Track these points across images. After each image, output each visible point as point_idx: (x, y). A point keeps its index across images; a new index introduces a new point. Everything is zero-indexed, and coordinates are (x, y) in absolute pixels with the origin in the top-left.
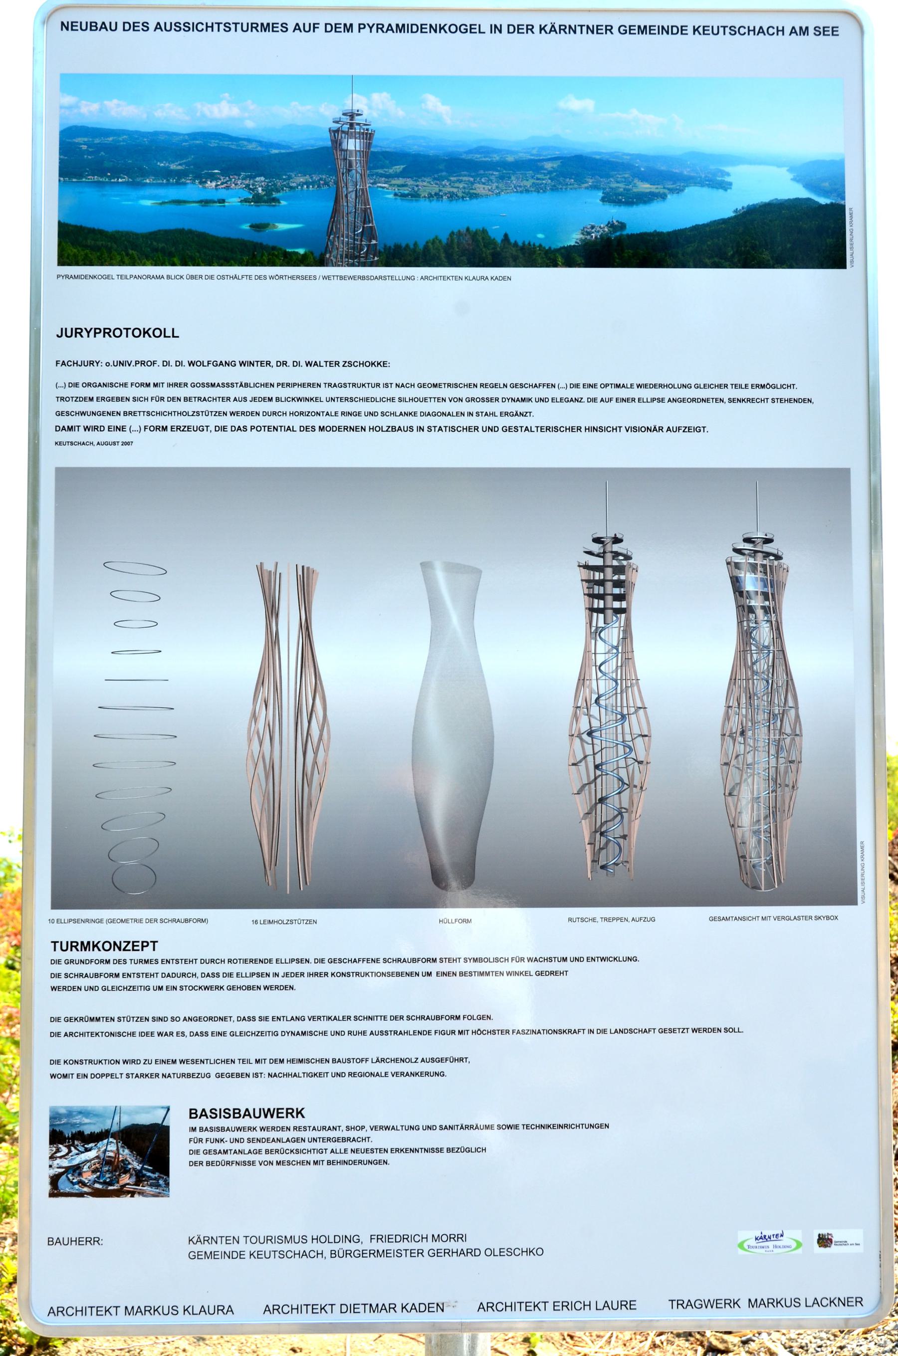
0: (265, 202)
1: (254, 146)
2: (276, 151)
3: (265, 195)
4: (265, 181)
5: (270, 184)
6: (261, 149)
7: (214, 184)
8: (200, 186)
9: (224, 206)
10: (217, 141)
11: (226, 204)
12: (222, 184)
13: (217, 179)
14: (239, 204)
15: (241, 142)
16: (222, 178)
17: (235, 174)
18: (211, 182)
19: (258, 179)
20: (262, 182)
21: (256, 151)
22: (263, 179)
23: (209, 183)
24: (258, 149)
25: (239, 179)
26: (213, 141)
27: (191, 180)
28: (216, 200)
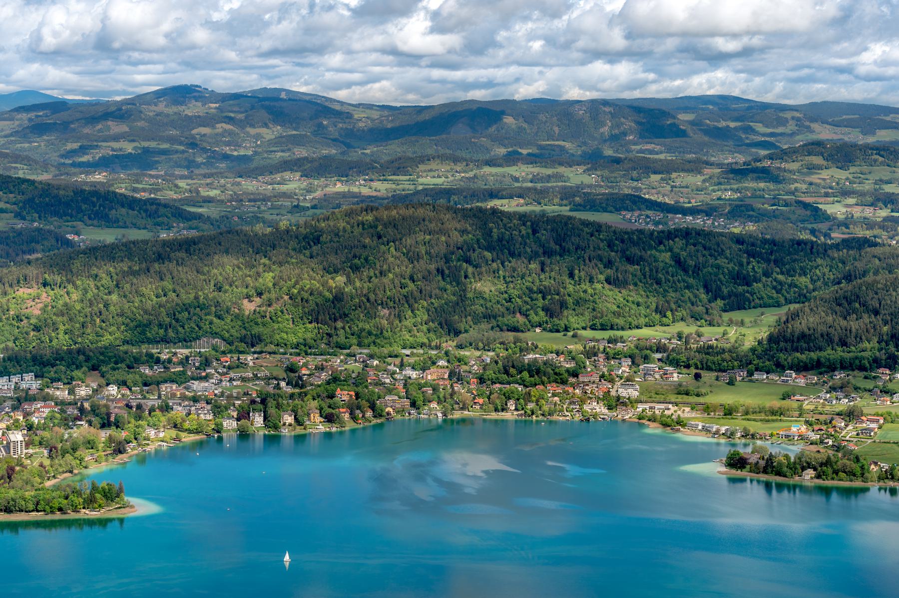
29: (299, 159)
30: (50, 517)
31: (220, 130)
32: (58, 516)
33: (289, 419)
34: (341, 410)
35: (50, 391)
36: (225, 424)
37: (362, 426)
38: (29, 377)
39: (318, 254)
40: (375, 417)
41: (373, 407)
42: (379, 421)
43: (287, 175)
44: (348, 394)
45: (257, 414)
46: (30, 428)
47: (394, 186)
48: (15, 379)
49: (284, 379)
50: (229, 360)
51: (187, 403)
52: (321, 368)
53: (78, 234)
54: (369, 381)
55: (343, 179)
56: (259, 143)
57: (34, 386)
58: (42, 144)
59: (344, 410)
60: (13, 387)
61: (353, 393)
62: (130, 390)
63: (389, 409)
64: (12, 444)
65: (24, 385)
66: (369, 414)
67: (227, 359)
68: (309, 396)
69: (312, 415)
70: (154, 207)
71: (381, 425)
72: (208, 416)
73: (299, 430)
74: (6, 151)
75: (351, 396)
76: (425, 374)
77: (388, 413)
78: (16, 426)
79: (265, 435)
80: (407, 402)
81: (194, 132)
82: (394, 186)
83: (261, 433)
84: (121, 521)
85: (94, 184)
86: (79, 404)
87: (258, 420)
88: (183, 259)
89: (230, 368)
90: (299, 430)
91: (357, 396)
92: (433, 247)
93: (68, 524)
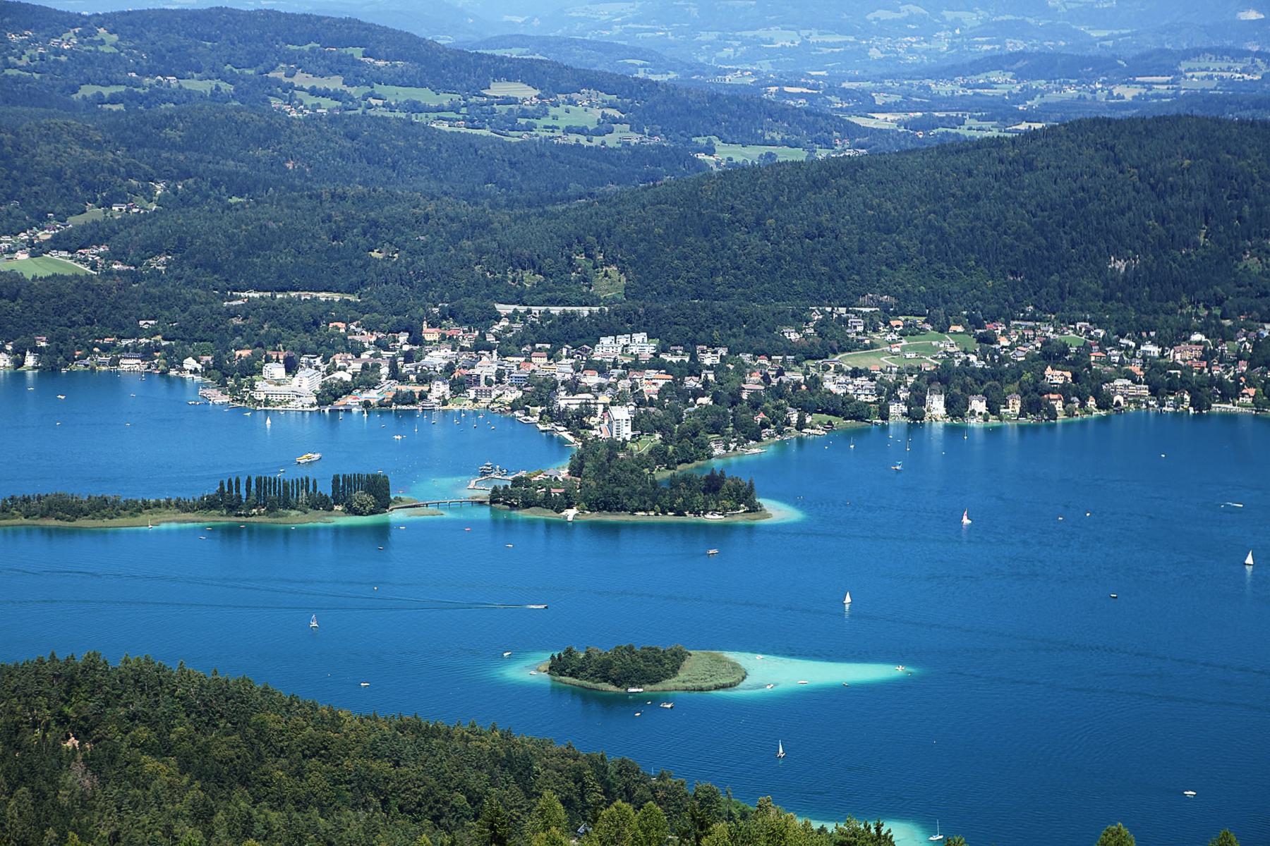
0: (654, 498)
1: (591, 117)
2: (747, 155)
3: (659, 456)
4: (656, 364)
5: (692, 382)
6: (635, 139)
7: (307, 382)
8: (219, 398)
9: (383, 531)
10: (335, 83)
11: (395, 516)
12: (366, 379)
13: (327, 348)
14: (485, 513)
15: (499, 89)
16: (368, 338)
17: (452, 314)
18: (291, 367)
19: (607, 348)
20: (637, 365)
21: (602, 154)
22: (643, 346)
23: (278, 371)
24: (611, 141)
25: (480, 346)
26: (302, 79)
27: (146, 354)
28: (326, 489)
29: (1011, 54)
30: (661, 518)
31: (906, 14)
32: (670, 517)
33: (979, 405)
34: (1052, 396)
35: (667, 358)
36: (892, 409)
37: (1079, 418)
38: (640, 337)
39: (1029, 185)
40: (1099, 407)
41: (1097, 394)
42: (1103, 413)
43: (995, 76)
44: (1062, 375)
45: (935, 397)
46: (641, 403)
47: (1143, 91)
48: (623, 340)
49: (975, 353)
50: (901, 324)
51: (842, 379)
52: (1023, 340)
53: (710, 151)
54: (1093, 358)
55: (1071, 81)
56: (957, 31)
57: (647, 349)
58: (670, 34)
59: (1056, 396)
60: (620, 350)
61: (1068, 374)
62: (770, 359)
63: (1118, 398)
64: (615, 424)
65: (634, 349)
66: (1091, 403)
67: (897, 322)
68: (1008, 377)
69: (1011, 402)
70: (812, 118)
71: (1108, 417)
72: (870, 396)
73: (993, 421)
74: (622, 43)
75: (1066, 378)
76: (1173, 351)
77: (1118, 403)
78: (619, 400)
79: (946, 426)
80: (1144, 390)
81: (870, 17)
82: (1143, 91)
83: (941, 424)
84: (750, 529)
85: (733, 87)
86: (703, 375)
87: (937, 405)
88: (846, 188)
89: (903, 334)
90: (993, 421)
91: (1075, 377)
92: (1194, 177)
93: (684, 527)
